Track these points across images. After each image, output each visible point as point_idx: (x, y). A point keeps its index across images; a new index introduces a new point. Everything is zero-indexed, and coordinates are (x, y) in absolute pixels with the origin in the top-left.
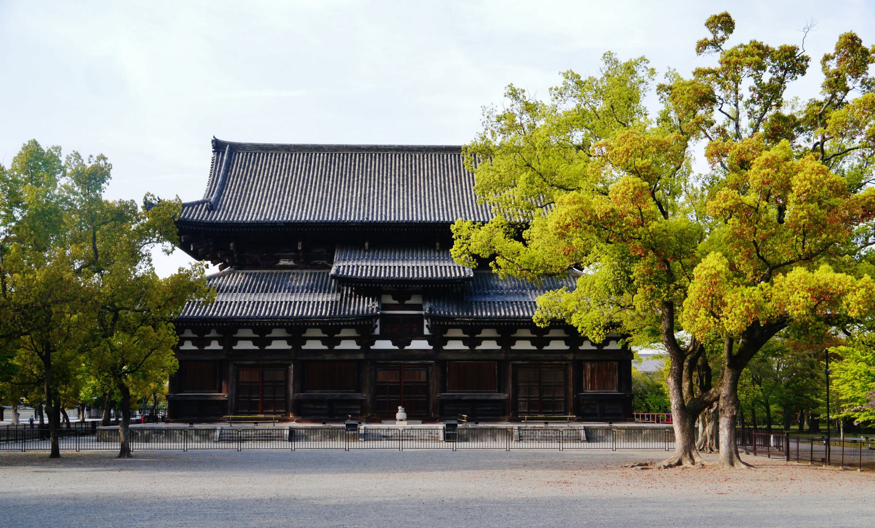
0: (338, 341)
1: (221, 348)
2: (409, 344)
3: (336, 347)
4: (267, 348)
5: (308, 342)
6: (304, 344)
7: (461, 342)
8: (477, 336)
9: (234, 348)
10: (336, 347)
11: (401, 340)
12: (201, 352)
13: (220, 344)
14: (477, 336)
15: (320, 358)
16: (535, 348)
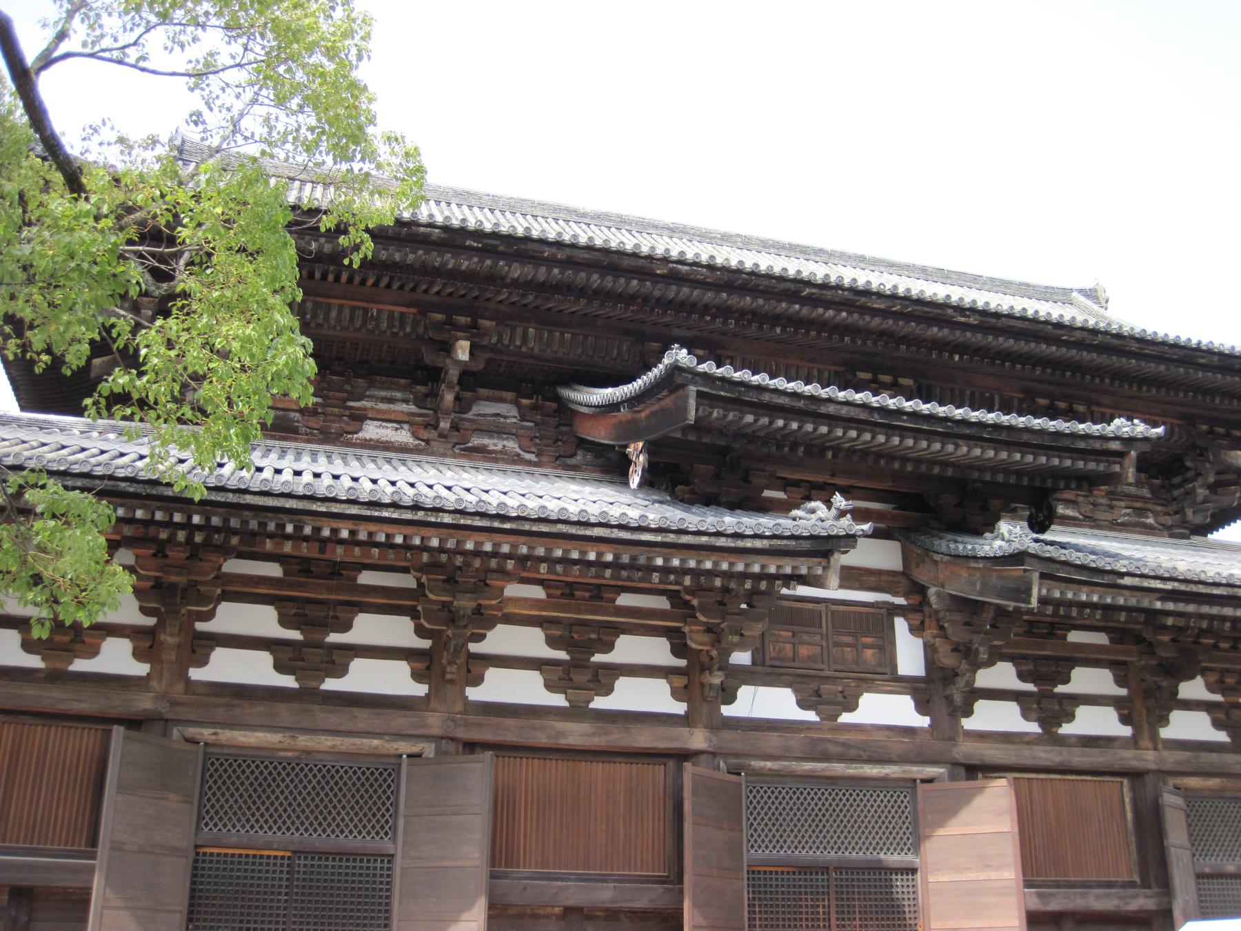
0: (605, 678)
1: (141, 669)
2: (852, 707)
3: (599, 703)
5: (492, 674)
6: (478, 681)
7: (1012, 708)
8: (1061, 689)
9: (195, 674)
10: (599, 703)
11: (827, 690)
12: (56, 677)
13: (138, 655)
14: (1061, 689)
15: (542, 739)
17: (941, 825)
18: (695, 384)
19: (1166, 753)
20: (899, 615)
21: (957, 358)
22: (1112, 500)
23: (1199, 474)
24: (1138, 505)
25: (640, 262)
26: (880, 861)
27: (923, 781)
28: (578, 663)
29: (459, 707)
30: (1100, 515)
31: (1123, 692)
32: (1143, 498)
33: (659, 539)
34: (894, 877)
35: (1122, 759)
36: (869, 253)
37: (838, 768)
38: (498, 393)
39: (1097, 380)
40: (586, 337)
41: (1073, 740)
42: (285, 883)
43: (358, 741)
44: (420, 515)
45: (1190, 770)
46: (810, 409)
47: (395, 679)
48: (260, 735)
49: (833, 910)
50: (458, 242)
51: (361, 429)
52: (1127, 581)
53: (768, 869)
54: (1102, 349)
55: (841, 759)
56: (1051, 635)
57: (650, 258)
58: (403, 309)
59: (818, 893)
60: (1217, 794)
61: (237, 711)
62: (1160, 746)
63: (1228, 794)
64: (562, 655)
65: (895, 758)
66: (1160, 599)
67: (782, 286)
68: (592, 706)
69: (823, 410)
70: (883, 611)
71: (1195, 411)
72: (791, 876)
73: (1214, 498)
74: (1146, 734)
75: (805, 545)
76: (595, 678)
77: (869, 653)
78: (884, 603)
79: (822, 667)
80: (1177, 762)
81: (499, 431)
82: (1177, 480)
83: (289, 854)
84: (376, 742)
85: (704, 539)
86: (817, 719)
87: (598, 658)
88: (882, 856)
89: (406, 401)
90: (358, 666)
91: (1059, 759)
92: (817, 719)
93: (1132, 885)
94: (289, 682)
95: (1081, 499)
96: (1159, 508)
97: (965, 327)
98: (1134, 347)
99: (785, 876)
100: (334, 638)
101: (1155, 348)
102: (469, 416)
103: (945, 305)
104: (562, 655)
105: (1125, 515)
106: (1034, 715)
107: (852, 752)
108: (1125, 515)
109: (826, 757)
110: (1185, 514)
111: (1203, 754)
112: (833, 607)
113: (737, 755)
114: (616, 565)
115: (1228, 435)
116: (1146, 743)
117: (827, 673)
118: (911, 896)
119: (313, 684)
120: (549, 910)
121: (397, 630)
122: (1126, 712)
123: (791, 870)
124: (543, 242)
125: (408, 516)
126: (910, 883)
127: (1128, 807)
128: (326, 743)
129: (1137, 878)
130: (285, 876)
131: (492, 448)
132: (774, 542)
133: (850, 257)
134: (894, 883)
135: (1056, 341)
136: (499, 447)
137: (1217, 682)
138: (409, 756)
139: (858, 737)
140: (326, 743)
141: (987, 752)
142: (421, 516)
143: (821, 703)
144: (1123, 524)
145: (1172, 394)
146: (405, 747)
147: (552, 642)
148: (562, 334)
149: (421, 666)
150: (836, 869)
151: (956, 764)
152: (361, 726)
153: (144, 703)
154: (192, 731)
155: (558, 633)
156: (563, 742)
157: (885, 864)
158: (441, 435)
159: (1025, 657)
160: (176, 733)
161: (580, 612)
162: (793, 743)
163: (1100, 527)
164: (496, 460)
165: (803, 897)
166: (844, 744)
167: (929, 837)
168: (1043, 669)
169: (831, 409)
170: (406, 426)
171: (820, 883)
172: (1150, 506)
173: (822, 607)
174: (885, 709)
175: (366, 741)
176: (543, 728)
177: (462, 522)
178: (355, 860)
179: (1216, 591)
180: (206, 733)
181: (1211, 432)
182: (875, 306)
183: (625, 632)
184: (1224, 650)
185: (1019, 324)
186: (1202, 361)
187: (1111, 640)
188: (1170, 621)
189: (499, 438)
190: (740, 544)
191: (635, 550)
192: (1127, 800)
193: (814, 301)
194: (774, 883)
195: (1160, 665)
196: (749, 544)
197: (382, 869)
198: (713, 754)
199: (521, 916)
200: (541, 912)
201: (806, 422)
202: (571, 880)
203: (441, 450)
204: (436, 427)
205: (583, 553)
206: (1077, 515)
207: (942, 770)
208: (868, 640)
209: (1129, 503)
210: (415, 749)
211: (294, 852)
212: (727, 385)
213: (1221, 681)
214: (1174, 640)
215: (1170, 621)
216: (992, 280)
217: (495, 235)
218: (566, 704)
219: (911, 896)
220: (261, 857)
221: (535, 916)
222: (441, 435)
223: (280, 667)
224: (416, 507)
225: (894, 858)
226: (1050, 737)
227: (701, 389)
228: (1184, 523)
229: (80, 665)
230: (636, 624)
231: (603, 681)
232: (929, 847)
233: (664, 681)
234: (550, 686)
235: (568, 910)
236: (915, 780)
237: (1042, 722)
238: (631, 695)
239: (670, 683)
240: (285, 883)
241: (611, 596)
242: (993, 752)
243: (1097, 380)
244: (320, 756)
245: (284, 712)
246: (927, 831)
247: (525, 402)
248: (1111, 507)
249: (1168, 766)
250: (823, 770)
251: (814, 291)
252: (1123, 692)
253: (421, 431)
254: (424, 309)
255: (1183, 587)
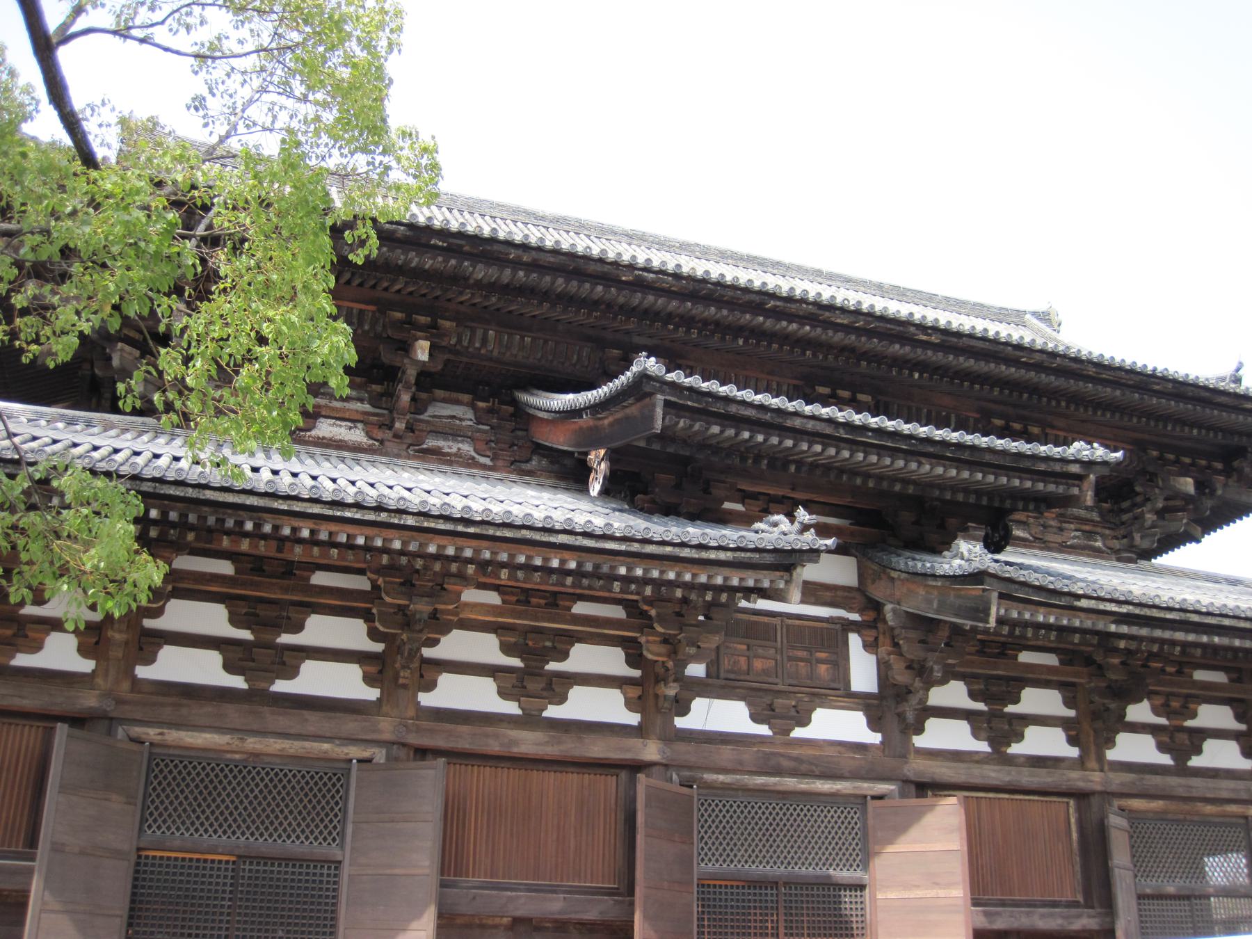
0: (559, 686)
1: (86, 666)
2: (804, 721)
3: (553, 712)
4: (281, 686)
5: (445, 679)
6: (430, 686)
7: (963, 727)
8: (1011, 709)
9: (142, 672)
10: (553, 712)
11: (780, 705)
14: (1011, 709)
15: (494, 747)
16: (1166, 759)
17: (890, 842)
18: (663, 393)
19: (1111, 775)
20: (853, 631)
21: (916, 375)
22: (1061, 522)
23: (1148, 499)
24: (1087, 528)
25: (607, 268)
26: (829, 877)
27: (874, 798)
28: (532, 671)
29: (411, 712)
30: (1050, 537)
31: (1071, 713)
32: (1093, 521)
33: (623, 548)
34: (842, 893)
35: (1069, 780)
36: (826, 267)
37: (790, 783)
38: (455, 395)
39: (1054, 403)
40: (546, 341)
41: (1022, 760)
42: (228, 888)
43: (307, 744)
44: (383, 517)
45: (1134, 791)
46: (776, 422)
47: (347, 682)
48: (208, 736)
49: (782, 925)
50: (423, 241)
51: (314, 427)
52: (1084, 603)
53: (718, 883)
54: (1061, 372)
55: (793, 773)
56: (1002, 655)
57: (616, 264)
58: (363, 306)
59: (766, 908)
60: (1161, 816)
61: (184, 711)
62: (1106, 768)
63: (1170, 816)
64: (516, 662)
65: (847, 774)
66: (1114, 622)
67: (747, 297)
68: (545, 714)
69: (789, 423)
70: (838, 626)
71: (1147, 437)
72: (741, 891)
73: (1161, 523)
74: (1093, 756)
75: (769, 559)
76: (549, 686)
77: (823, 668)
78: (839, 618)
79: (776, 681)
80: (1122, 784)
81: (454, 434)
82: (1126, 505)
83: (233, 859)
84: (326, 746)
85: (668, 549)
86: (770, 733)
87: (552, 666)
88: (831, 871)
89: (361, 400)
90: (310, 668)
91: (1007, 779)
92: (770, 733)
93: (1075, 904)
94: (238, 682)
95: (1032, 520)
96: (1107, 532)
97: (926, 345)
98: (1092, 371)
99: (735, 890)
100: (286, 639)
101: (1111, 373)
102: (424, 417)
103: (907, 323)
104: (516, 662)
105: (1075, 537)
106: (984, 734)
107: (804, 767)
108: (1075, 537)
109: (778, 772)
110: (1133, 538)
111: (1148, 777)
112: (790, 622)
113: (690, 768)
114: (579, 573)
115: (1177, 461)
116: (1093, 764)
117: (781, 687)
118: (859, 913)
119: (263, 685)
120: (497, 921)
121: (350, 633)
122: (1073, 733)
123: (741, 884)
124: (509, 243)
125: (371, 516)
126: (859, 900)
127: (1074, 827)
128: (275, 745)
129: (1080, 898)
130: (229, 881)
131: (447, 450)
132: (738, 554)
133: (807, 271)
134: (843, 899)
135: (1015, 362)
136: (454, 450)
137: (1163, 705)
138: (359, 761)
139: (810, 752)
140: (275, 745)
141: (938, 771)
142: (384, 517)
143: (775, 717)
144: (1071, 547)
145: (1126, 419)
146: (355, 752)
147: (506, 649)
148: (522, 338)
149: (373, 669)
150: (785, 884)
151: (906, 781)
152: (311, 729)
153: (89, 701)
154: (137, 731)
155: (513, 640)
156: (515, 750)
157: (834, 880)
158: (396, 436)
159: (975, 676)
160: (120, 732)
161: (537, 620)
162: (746, 757)
163: (1049, 549)
164: (450, 463)
165: (752, 911)
166: (796, 759)
167: (879, 853)
168: (994, 689)
169: (797, 423)
170: (360, 425)
171: (769, 898)
172: (1099, 530)
173: (777, 621)
174: (838, 725)
175: (315, 745)
176: (496, 736)
177: (426, 524)
178: (301, 866)
179: (1169, 616)
180: (152, 733)
181: (1161, 458)
182: (839, 321)
183: (580, 641)
184: (1170, 674)
185: (980, 344)
186: (1157, 387)
187: (1061, 662)
188: (1122, 644)
189: (454, 440)
190: (704, 555)
191: (598, 559)
192: (1073, 820)
193: (777, 314)
194: (723, 897)
195: (1109, 687)
196: (712, 555)
197: (329, 875)
198: (666, 766)
199: (469, 926)
200: (490, 922)
201: (772, 435)
202: (520, 890)
203: (396, 451)
204: (390, 427)
205: (546, 560)
206: (1028, 536)
207: (893, 787)
208: (822, 655)
209: (1079, 526)
210: (366, 754)
211: (239, 857)
212: (694, 396)
213: (1166, 705)
214: (1123, 663)
215: (1122, 644)
216: (948, 299)
217: (461, 235)
218: (519, 712)
219: (859, 913)
220: (205, 861)
221: (483, 926)
222: (396, 436)
223: (229, 667)
224: (379, 508)
225: (843, 874)
226: (999, 756)
227: (668, 398)
228: (1131, 547)
229: (281, 686)
230: (591, 633)
231: (557, 690)
232: (878, 863)
233: (618, 691)
234: (503, 694)
235: (517, 921)
236: (865, 797)
237: (992, 742)
238: (584, 705)
239: (624, 694)
240: (228, 888)
241: (567, 603)
242: (944, 770)
243: (1054, 403)
244: (267, 759)
245: (233, 713)
246: (877, 848)
247: (481, 404)
248: (1061, 529)
249: (1113, 788)
250: (775, 784)
251: (778, 303)
252: (1071, 713)
253: (375, 431)
254: (384, 306)
255: (1137, 611)
